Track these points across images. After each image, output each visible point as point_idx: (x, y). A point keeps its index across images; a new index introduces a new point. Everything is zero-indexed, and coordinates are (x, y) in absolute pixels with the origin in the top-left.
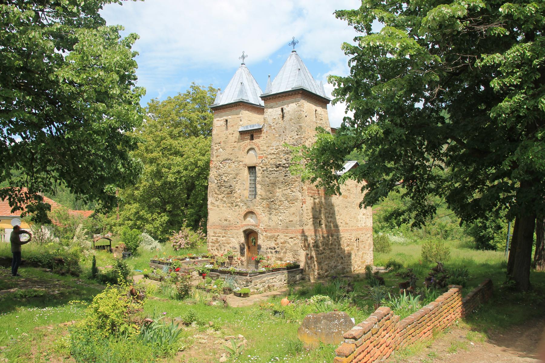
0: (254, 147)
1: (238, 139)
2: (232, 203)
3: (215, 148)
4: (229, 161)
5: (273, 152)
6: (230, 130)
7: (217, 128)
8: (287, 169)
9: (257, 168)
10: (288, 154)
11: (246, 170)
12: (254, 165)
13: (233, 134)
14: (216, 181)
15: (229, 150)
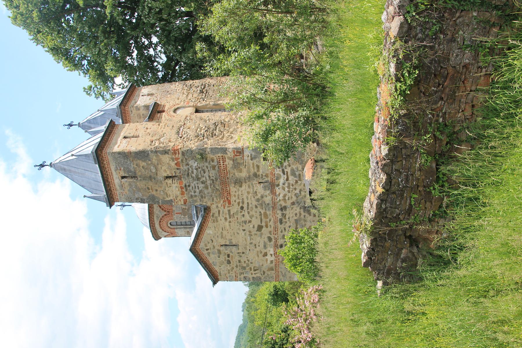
0: (173, 108)
1: (157, 122)
2: (237, 122)
3: (157, 145)
4: (181, 129)
5: (185, 96)
6: (141, 133)
7: (129, 146)
8: (207, 86)
9: (199, 105)
10: (191, 88)
11: (198, 114)
12: (195, 110)
13: (147, 129)
14: (206, 140)
15: (167, 130)
